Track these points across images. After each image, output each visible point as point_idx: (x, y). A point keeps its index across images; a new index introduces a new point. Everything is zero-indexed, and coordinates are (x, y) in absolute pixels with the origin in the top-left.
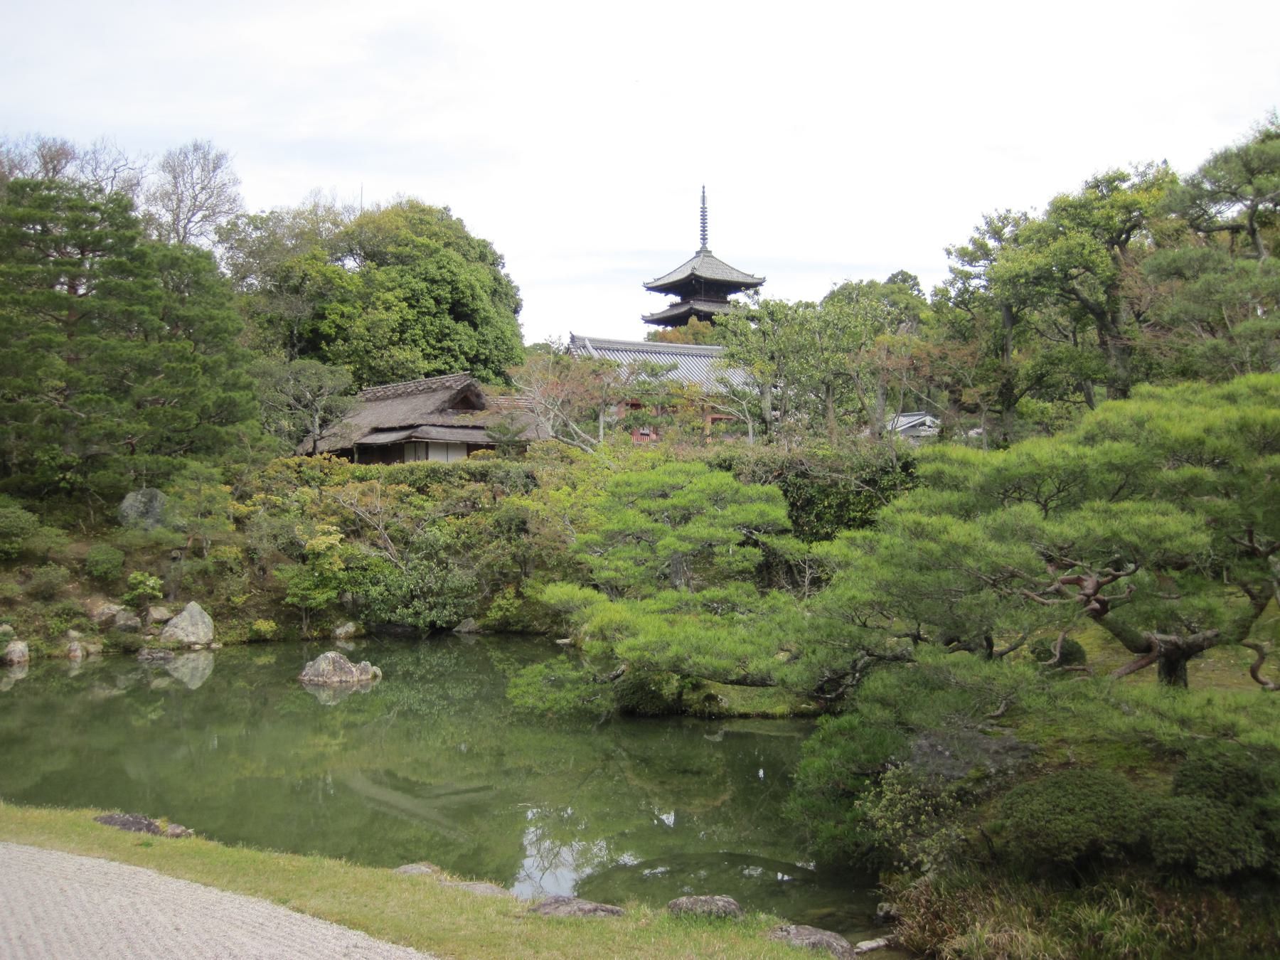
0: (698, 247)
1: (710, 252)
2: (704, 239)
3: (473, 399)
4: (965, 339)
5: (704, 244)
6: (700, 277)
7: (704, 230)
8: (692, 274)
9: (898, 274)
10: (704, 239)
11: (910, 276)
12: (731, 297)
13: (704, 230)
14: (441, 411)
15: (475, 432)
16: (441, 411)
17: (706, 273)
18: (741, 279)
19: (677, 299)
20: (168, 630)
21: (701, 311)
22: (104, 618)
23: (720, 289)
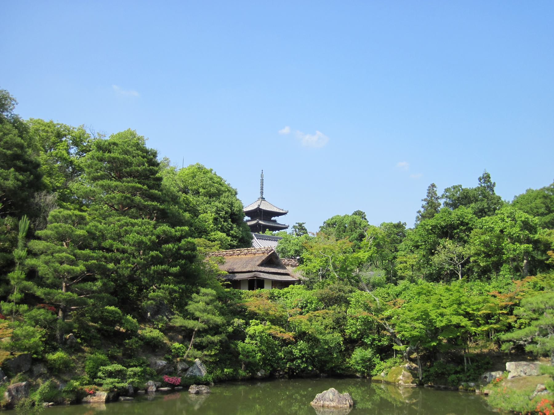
0: (260, 196)
1: (264, 199)
2: (262, 193)
3: (274, 260)
4: (394, 241)
5: (262, 195)
6: (261, 209)
7: (262, 189)
8: (258, 208)
9: (357, 211)
10: (262, 193)
11: (362, 212)
12: (273, 218)
13: (262, 189)
14: (262, 265)
15: (277, 276)
16: (262, 265)
17: (263, 207)
18: (278, 211)
19: (249, 218)
20: (188, 374)
21: (261, 224)
22: (160, 368)
23: (268, 215)
